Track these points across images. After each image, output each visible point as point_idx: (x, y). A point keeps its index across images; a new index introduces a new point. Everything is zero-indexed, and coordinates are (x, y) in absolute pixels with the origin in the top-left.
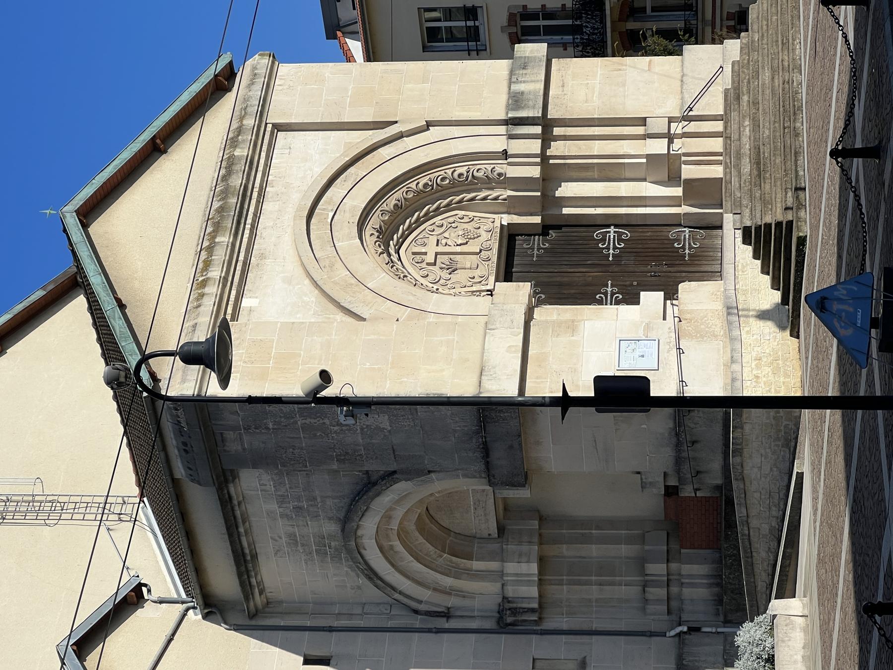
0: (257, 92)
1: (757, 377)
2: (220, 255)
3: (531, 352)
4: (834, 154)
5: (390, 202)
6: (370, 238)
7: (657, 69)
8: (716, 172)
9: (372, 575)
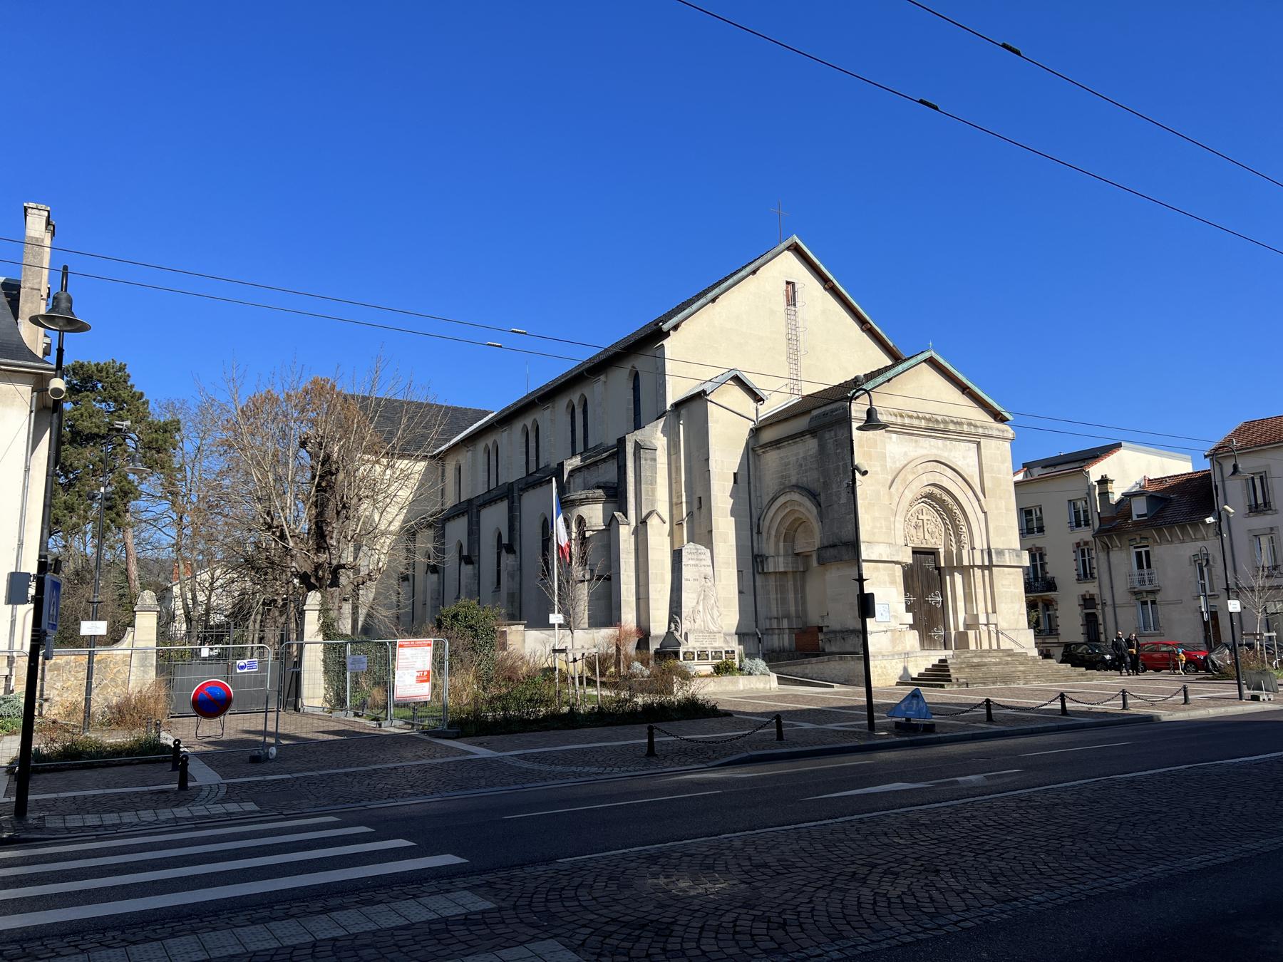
0: (995, 433)
2: (916, 422)
4: (988, 701)
5: (946, 497)
6: (928, 489)
8: (972, 646)
9: (774, 499)
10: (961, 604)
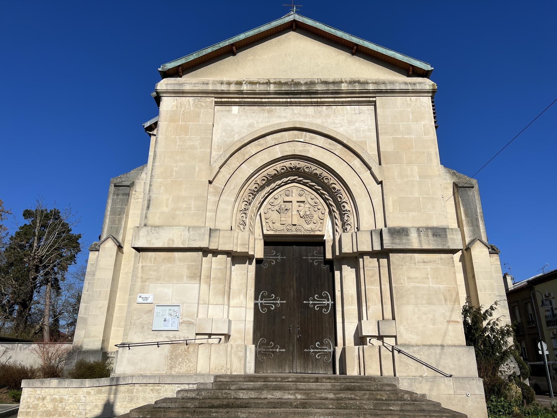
0: (397, 87)
1: (44, 399)
2: (258, 88)
3: (176, 254)
5: (288, 164)
7: (451, 327)
10: (351, 308)
